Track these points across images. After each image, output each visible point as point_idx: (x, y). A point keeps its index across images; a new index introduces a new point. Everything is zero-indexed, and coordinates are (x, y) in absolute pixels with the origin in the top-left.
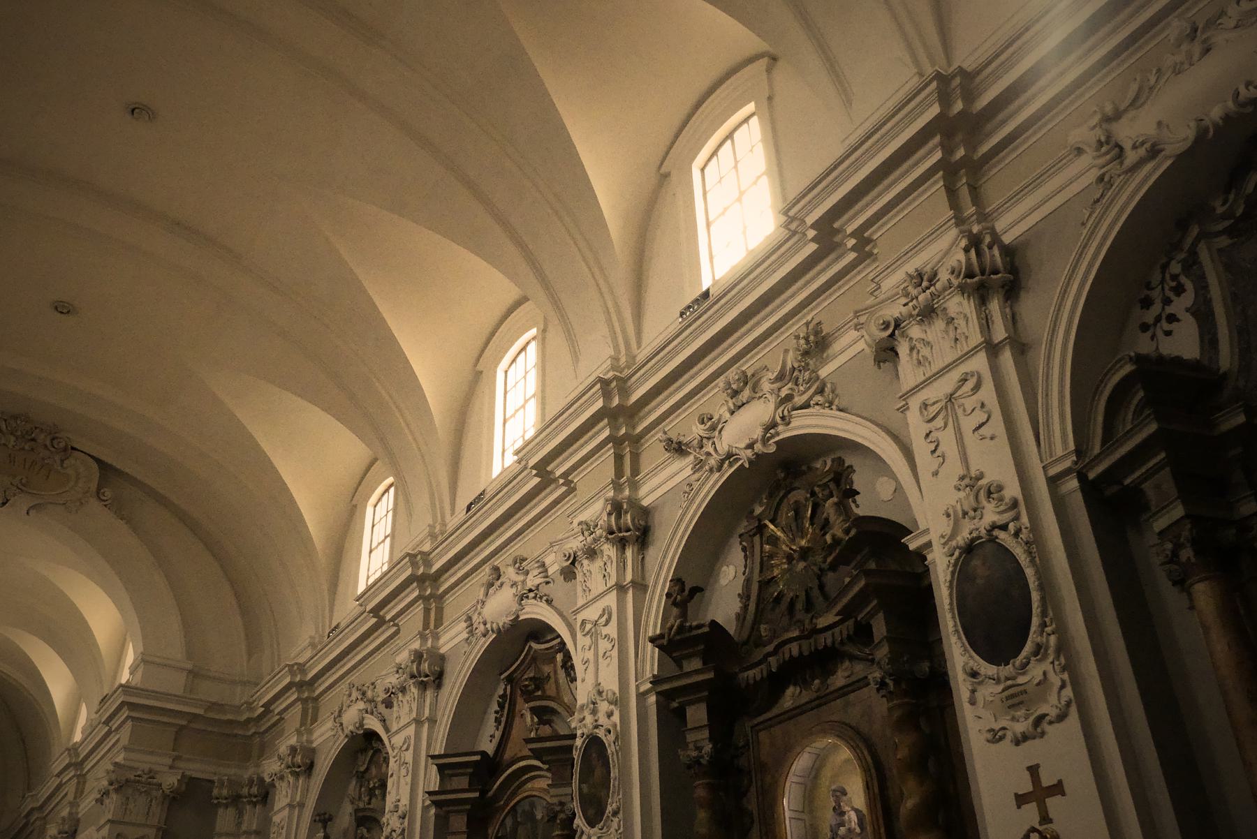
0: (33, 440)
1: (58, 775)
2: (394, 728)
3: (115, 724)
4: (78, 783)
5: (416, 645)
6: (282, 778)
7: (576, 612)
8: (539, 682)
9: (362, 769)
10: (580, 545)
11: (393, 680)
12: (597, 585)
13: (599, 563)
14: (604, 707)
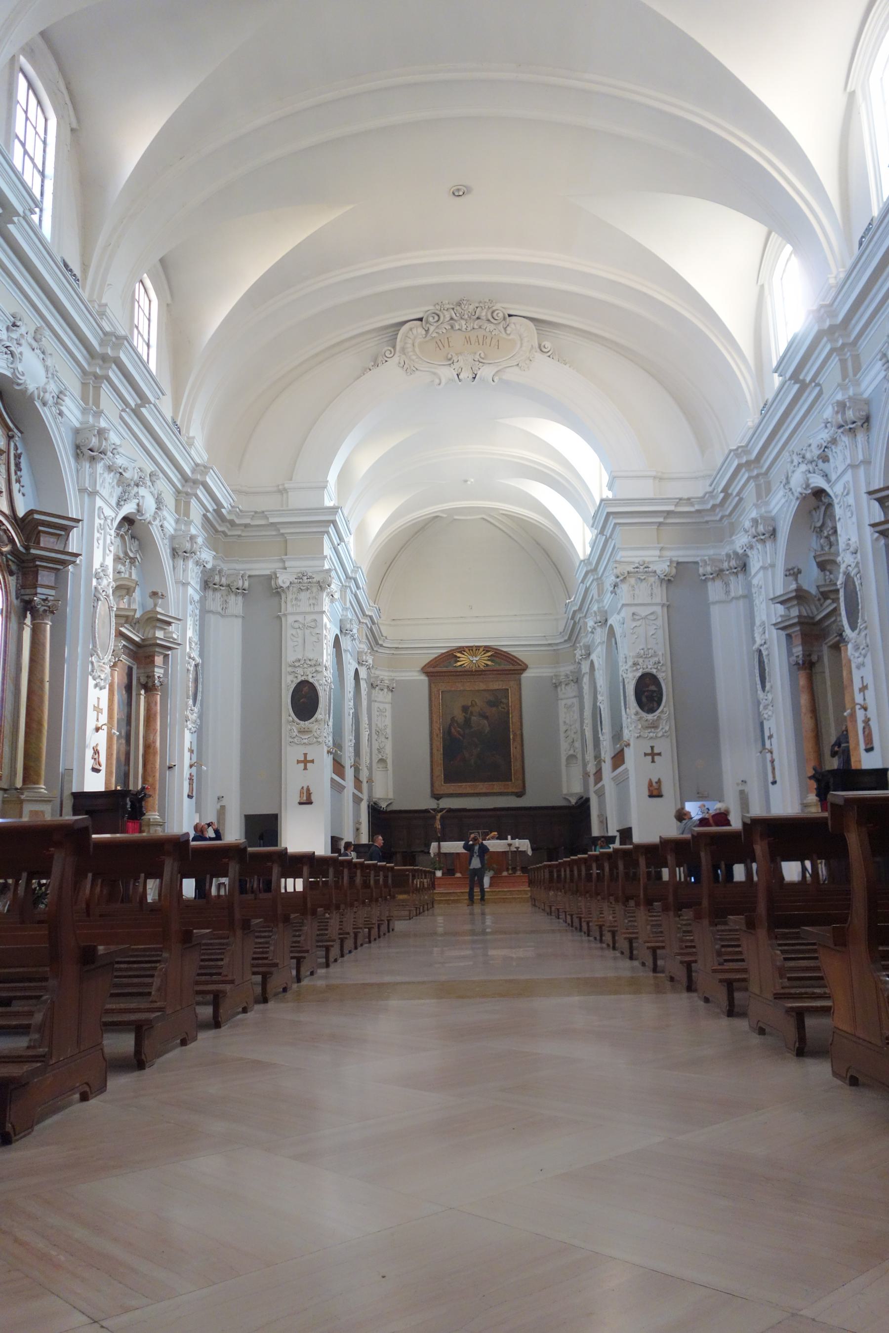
0: (478, 318)
1: (582, 582)
2: (833, 477)
3: (608, 532)
4: (598, 584)
5: (839, 397)
6: (751, 547)
9: (819, 524)
11: (824, 436)
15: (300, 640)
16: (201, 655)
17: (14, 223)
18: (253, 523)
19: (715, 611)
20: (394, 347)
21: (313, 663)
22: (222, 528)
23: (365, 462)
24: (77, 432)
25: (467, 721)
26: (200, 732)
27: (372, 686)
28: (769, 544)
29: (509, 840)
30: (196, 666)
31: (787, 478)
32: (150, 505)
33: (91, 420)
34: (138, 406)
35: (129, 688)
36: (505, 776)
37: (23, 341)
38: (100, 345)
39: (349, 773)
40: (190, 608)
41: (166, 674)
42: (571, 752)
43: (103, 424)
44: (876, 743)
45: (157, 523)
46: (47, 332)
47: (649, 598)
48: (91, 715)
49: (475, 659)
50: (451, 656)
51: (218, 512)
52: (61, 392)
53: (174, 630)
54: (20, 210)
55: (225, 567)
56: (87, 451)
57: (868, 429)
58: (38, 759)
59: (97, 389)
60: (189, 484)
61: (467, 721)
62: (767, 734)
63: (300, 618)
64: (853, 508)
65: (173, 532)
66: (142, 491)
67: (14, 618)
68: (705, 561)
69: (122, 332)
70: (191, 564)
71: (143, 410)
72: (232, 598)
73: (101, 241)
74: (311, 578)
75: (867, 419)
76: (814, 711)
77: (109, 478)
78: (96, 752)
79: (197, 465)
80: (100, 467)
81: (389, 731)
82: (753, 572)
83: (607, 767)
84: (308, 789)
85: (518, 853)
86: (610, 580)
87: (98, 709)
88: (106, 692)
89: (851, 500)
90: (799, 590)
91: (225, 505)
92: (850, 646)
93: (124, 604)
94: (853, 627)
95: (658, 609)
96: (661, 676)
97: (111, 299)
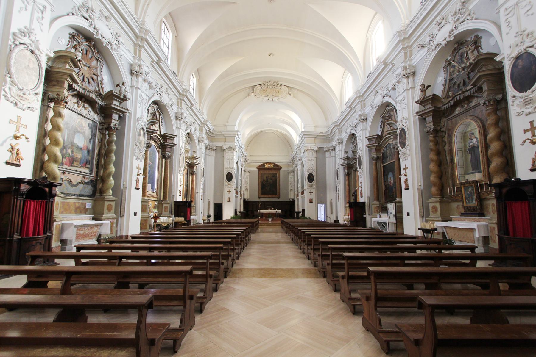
5: (360, 113)
7: (396, 98)
8: (390, 117)
11: (356, 122)
12: (401, 90)
13: (401, 84)
14: (404, 121)
19: (327, 159)
22: (211, 135)
23: (245, 119)
24: (176, 113)
25: (267, 180)
26: (204, 185)
27: (245, 171)
35: (187, 174)
39: (239, 193)
43: (182, 111)
44: (363, 196)
47: (312, 155)
48: (179, 182)
50: (263, 165)
51: (209, 131)
53: (198, 160)
55: (211, 144)
58: (166, 194)
59: (181, 103)
60: (203, 124)
61: (267, 181)
66: (191, 127)
69: (188, 89)
70: (203, 144)
75: (366, 119)
76: (349, 185)
77: (184, 124)
80: (182, 122)
83: (300, 194)
85: (278, 213)
86: (303, 150)
87: (180, 181)
89: (361, 138)
90: (347, 157)
93: (187, 155)
94: (360, 168)
96: (314, 174)
97: (185, 80)
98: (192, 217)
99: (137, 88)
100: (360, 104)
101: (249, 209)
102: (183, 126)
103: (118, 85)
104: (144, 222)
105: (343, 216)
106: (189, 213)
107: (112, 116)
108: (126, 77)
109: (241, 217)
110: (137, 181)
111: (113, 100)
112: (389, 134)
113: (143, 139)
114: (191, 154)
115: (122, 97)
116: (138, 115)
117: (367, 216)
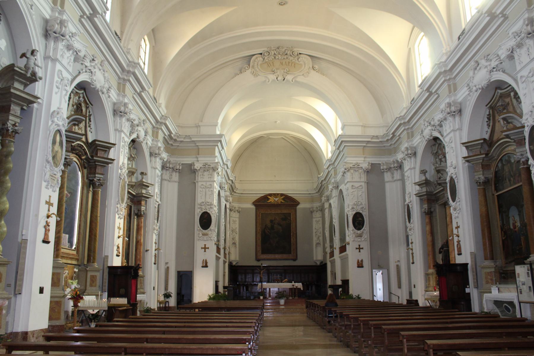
0: (286, 54)
1: (327, 168)
2: (445, 135)
3: (341, 149)
6: (405, 159)
8: (505, 107)
9: (435, 152)
10: (515, 43)
12: (525, 59)
13: (525, 49)
15: (204, 194)
16: (161, 200)
17: (97, 17)
18: (184, 140)
19: (388, 186)
20: (249, 65)
21: (209, 204)
22: (171, 144)
25: (272, 227)
26: (159, 235)
27: (231, 210)
28: (413, 159)
29: (293, 283)
30: (159, 205)
31: (422, 131)
32: (142, 134)
33: (121, 99)
34: (141, 92)
35: (129, 215)
36: (289, 252)
37: (96, 67)
38: (127, 66)
40: (157, 179)
41: (146, 209)
42: (318, 242)
43: (126, 101)
45: (145, 142)
46: (106, 63)
48: (117, 230)
49: (276, 199)
50: (265, 198)
51: (170, 136)
52: (110, 87)
54: (100, 12)
55: (172, 160)
56: (119, 112)
57: (461, 115)
59: (124, 86)
60: (159, 124)
61: (272, 227)
62: (410, 241)
63: (204, 183)
64: (454, 149)
65: (150, 145)
66: (140, 128)
67: (85, 188)
68: (383, 164)
69: (136, 61)
70: (158, 159)
71: (143, 94)
72: (174, 173)
73: (129, 22)
74: (210, 165)
75: (460, 111)
76: (432, 233)
78: (118, 247)
79: (163, 116)
80: (124, 119)
81: (237, 230)
82: (405, 170)
83: (337, 252)
84: (206, 261)
88: (123, 220)
89: (453, 145)
90: (426, 180)
91: (173, 132)
92: (451, 208)
94: (454, 200)
95: (363, 184)
96: (364, 214)
97: (132, 46)
98: (139, 297)
99: (55, 60)
100: (446, 84)
101: (239, 281)
102: (126, 127)
103: (23, 55)
104: (55, 306)
105: (424, 293)
106: (134, 288)
107: (9, 109)
108: (37, 42)
109: (225, 298)
110: (47, 226)
111: (13, 79)
112: (507, 136)
113: (60, 150)
114: (137, 178)
115: (29, 75)
116: (53, 108)
117: (472, 290)
